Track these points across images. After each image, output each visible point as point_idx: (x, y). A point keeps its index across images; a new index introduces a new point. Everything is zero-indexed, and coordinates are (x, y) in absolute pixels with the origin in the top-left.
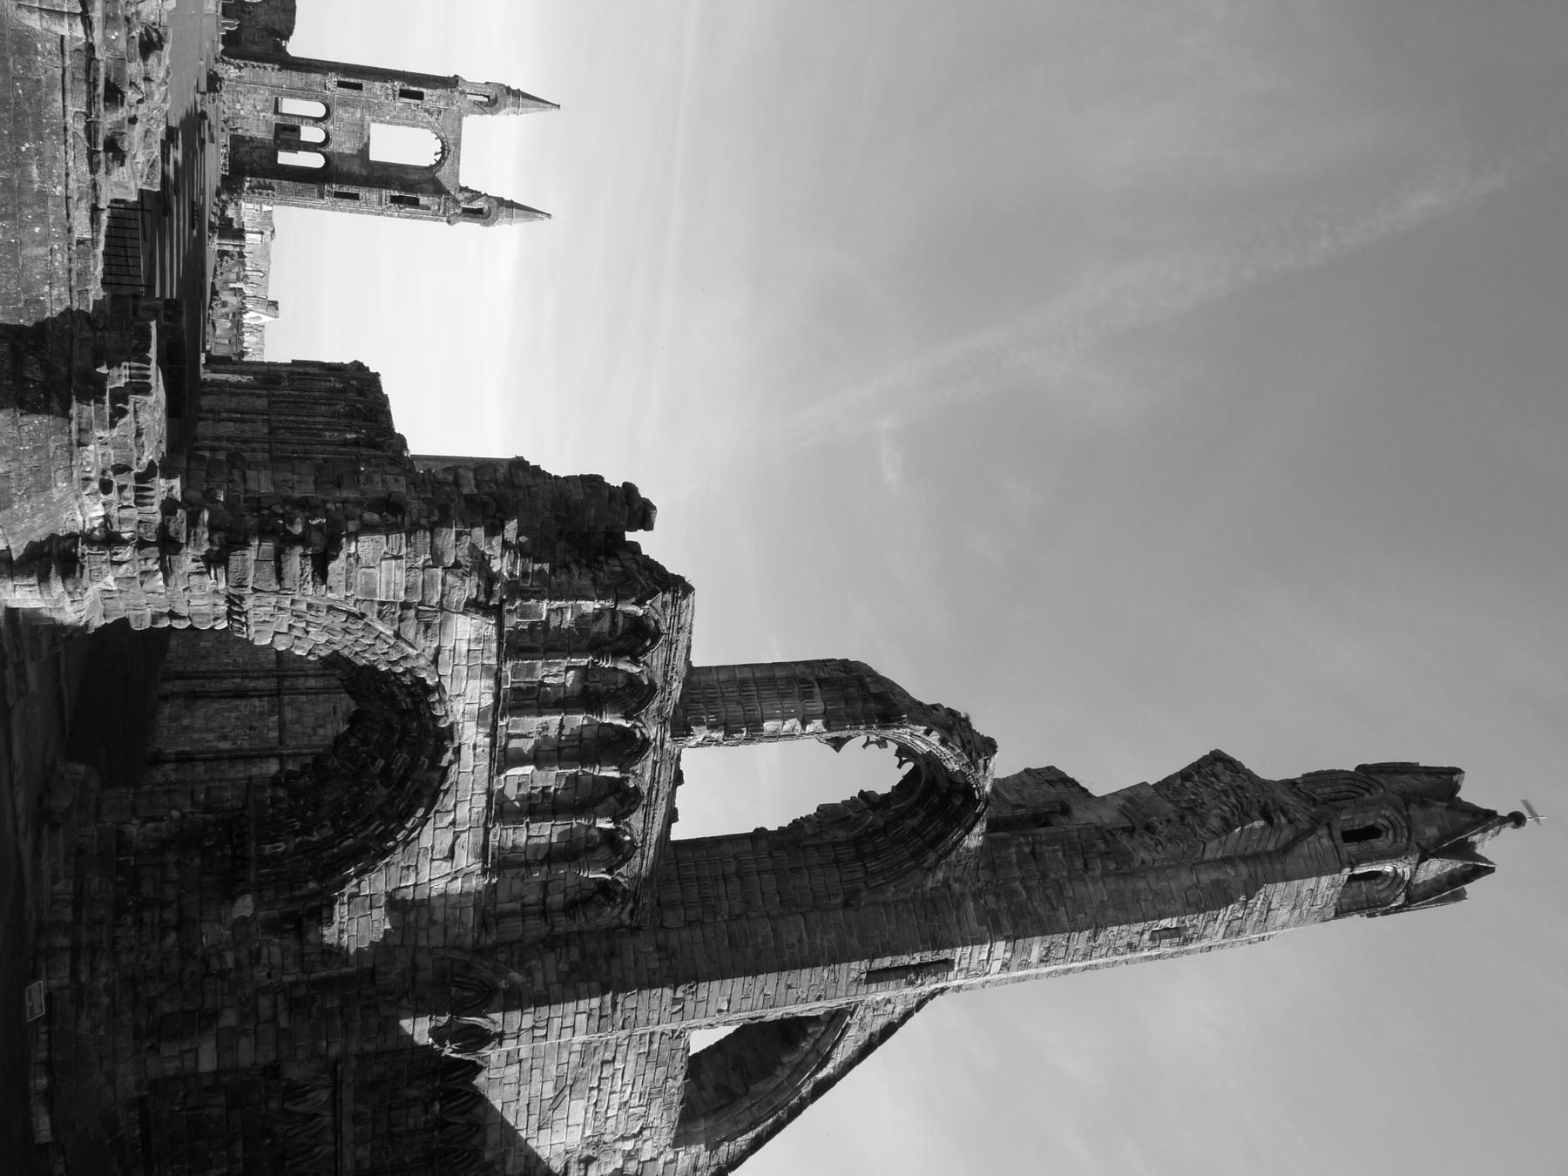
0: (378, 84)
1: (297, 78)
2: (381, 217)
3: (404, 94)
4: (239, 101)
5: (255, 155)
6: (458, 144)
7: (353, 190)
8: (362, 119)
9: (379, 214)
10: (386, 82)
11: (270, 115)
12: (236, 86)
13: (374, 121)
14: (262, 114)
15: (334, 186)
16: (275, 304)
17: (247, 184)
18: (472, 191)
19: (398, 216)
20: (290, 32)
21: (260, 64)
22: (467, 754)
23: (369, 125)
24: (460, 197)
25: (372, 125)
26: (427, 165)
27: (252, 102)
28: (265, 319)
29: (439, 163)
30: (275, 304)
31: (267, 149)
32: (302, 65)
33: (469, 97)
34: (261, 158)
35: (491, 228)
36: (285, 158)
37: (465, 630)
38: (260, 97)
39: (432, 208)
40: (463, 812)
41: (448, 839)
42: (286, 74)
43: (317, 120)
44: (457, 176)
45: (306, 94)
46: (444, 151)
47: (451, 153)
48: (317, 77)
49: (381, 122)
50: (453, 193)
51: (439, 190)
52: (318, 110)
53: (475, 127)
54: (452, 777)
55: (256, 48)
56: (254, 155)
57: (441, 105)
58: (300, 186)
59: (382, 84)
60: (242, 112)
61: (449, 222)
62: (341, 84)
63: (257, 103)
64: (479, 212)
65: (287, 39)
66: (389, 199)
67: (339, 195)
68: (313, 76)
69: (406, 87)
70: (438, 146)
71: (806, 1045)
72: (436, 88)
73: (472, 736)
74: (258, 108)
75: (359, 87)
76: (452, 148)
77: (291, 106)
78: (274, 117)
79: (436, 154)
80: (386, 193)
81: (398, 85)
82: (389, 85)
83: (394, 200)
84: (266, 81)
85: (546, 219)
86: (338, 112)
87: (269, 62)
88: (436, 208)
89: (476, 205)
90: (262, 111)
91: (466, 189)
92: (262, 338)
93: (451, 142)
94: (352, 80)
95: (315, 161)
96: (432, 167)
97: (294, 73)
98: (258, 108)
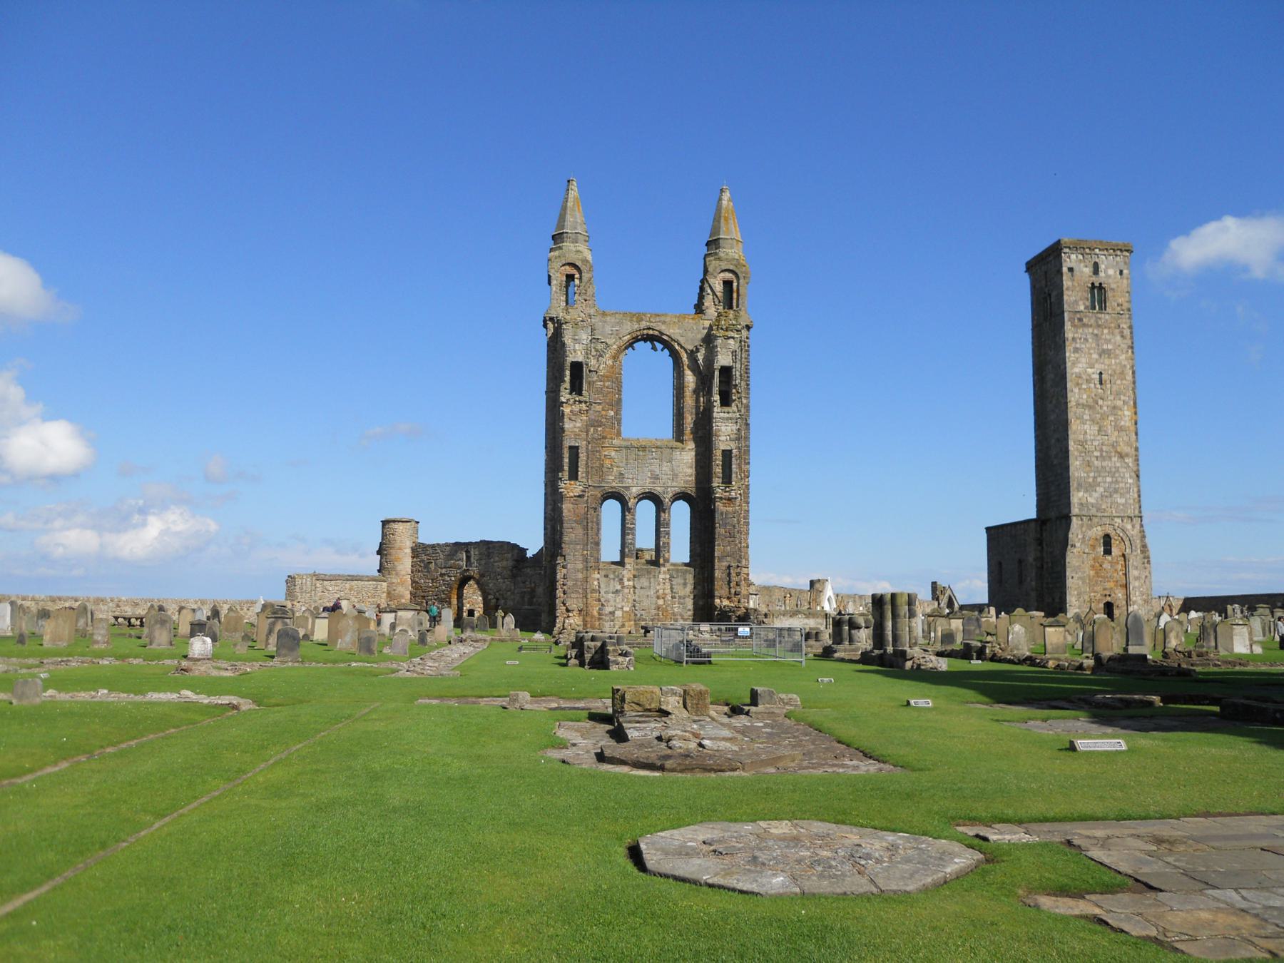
0: (568, 425)
1: (572, 534)
2: (750, 421)
3: (576, 388)
4: (612, 613)
7: (718, 456)
9: (748, 425)
10: (563, 415)
11: (627, 573)
12: (592, 616)
13: (619, 434)
14: (626, 583)
15: (715, 485)
17: (726, 602)
18: (701, 297)
19: (747, 398)
20: (515, 547)
21: (559, 585)
23: (624, 440)
24: (711, 309)
25: (625, 434)
26: (670, 360)
27: (610, 596)
28: (829, 592)
30: (812, 583)
31: (672, 576)
32: (554, 528)
34: (685, 584)
36: (680, 549)
38: (602, 586)
39: (733, 348)
42: (567, 549)
43: (625, 508)
45: (591, 526)
46: (652, 338)
47: (652, 325)
48: (567, 507)
50: (707, 324)
52: (611, 509)
55: (540, 590)
56: (682, 594)
57: (585, 336)
58: (720, 531)
59: (566, 420)
60: (626, 609)
62: (574, 476)
63: (612, 589)
64: (728, 284)
65: (524, 551)
66: (726, 409)
67: (727, 480)
68: (565, 513)
69: (567, 385)
72: (563, 345)
74: (619, 587)
75: (574, 450)
76: (644, 324)
77: (610, 550)
78: (627, 566)
79: (654, 348)
80: (718, 412)
81: (565, 396)
82: (567, 410)
83: (726, 401)
86: (612, 482)
87: (554, 573)
88: (731, 341)
89: (719, 288)
90: (621, 580)
91: (699, 308)
92: (849, 596)
93: (636, 327)
94: (566, 460)
95: (680, 515)
96: (675, 355)
97: (566, 538)
98: (619, 587)
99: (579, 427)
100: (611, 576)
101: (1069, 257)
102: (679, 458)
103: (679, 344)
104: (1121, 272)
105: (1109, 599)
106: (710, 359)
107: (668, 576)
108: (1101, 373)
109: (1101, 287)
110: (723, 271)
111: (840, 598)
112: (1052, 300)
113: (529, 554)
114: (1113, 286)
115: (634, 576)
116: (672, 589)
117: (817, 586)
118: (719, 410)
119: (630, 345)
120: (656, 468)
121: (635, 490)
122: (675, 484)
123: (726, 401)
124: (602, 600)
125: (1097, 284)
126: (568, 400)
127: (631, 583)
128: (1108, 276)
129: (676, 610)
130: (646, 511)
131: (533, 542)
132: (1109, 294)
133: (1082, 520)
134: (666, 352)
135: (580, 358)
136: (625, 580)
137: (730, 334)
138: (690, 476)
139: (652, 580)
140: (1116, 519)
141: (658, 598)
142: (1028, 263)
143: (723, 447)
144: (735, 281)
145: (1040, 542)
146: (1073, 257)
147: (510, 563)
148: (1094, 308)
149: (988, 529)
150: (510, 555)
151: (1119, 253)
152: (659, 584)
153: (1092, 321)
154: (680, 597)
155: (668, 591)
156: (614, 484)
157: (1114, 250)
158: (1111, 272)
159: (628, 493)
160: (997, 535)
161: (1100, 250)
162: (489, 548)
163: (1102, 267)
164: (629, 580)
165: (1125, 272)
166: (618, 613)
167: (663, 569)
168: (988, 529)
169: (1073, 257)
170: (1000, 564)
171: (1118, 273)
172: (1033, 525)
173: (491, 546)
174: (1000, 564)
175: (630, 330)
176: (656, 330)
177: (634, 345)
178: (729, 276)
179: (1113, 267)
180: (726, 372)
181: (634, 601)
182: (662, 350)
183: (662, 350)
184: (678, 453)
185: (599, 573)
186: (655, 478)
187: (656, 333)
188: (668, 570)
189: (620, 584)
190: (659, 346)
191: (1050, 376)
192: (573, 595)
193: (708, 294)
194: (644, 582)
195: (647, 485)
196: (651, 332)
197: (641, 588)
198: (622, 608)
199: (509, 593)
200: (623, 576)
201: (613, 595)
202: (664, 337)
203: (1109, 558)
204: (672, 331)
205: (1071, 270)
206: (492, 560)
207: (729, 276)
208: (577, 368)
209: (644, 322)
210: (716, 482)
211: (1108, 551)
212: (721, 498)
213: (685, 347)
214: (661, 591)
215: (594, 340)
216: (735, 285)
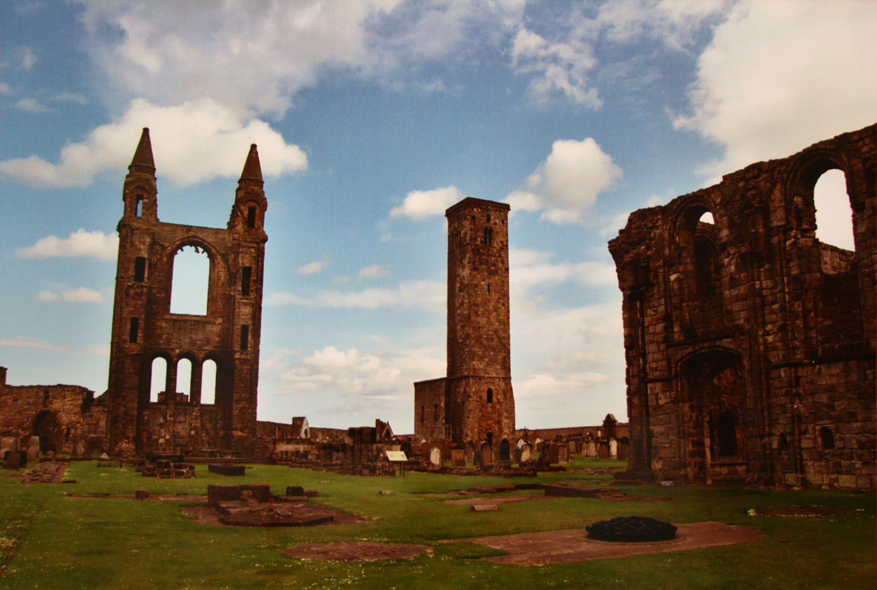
3: (139, 277)
4: (157, 440)
5: (209, 426)
6: (189, 228)
8: (167, 321)
14: (168, 418)
16: (295, 419)
17: (240, 433)
20: (83, 390)
26: (208, 260)
27: (157, 428)
29: (206, 249)
30: (295, 419)
33: (139, 214)
35: (268, 201)
36: (208, 396)
44: (217, 231)
49: (169, 303)
51: (236, 248)
53: (167, 214)
60: (168, 437)
61: (265, 240)
62: (133, 339)
64: (252, 211)
65: (92, 393)
67: (244, 346)
70: (189, 250)
74: (162, 421)
76: (191, 233)
79: (197, 251)
84: (135, 412)
85: (258, 149)
88: (253, 250)
89: (246, 213)
90: (165, 418)
91: (231, 224)
93: (186, 235)
95: (210, 368)
96: (211, 256)
98: (162, 421)
99: (140, 305)
100: (158, 413)
101: (473, 210)
102: (210, 328)
103: (216, 250)
104: (503, 223)
105: (490, 431)
106: (236, 260)
107: (199, 414)
108: (489, 286)
110: (251, 200)
111: (313, 430)
112: (462, 236)
113: (96, 396)
114: (498, 230)
115: (175, 414)
116: (202, 423)
117: (299, 423)
118: (241, 297)
119: (180, 247)
120: (194, 337)
121: (177, 351)
122: (206, 348)
123: (245, 292)
124: (150, 430)
125: (489, 228)
126: (134, 284)
127: (172, 419)
128: (495, 224)
129: (204, 438)
130: (184, 367)
131: (99, 386)
132: (494, 235)
133: (475, 379)
134: (206, 254)
136: (168, 416)
137: (251, 245)
138: (218, 342)
139: (187, 416)
140: (496, 380)
141: (191, 429)
142: (447, 211)
143: (242, 323)
144: (258, 208)
145: (447, 394)
146: (475, 210)
147: (80, 402)
148: (485, 243)
149: (416, 384)
150: (81, 397)
151: (502, 210)
152: (192, 419)
153: (485, 252)
154: (207, 429)
155: (199, 425)
156: (162, 347)
157: (500, 208)
158: (497, 221)
159: (173, 353)
160: (420, 387)
161: (491, 207)
162: (64, 391)
164: (170, 416)
165: (505, 222)
166: (161, 441)
167: (195, 409)
168: (416, 384)
169: (475, 210)
170: (423, 408)
171: (501, 222)
172: (444, 382)
173: (66, 389)
174: (423, 408)
175: (181, 237)
176: (200, 238)
177: (184, 248)
178: (253, 204)
179: (499, 218)
180: (247, 271)
181: (174, 431)
182: (203, 252)
183: (203, 252)
184: (210, 326)
185: (148, 411)
186: (193, 343)
187: (200, 240)
188: (200, 410)
189: (164, 419)
190: (201, 250)
191: (458, 285)
192: (129, 427)
193: (238, 216)
194: (181, 418)
195: (186, 347)
196: (196, 240)
197: (180, 422)
198: (164, 437)
199: (78, 425)
200: (167, 414)
201: (159, 427)
202: (205, 243)
203: (490, 404)
204: (210, 239)
205: (473, 218)
206: (66, 400)
207: (253, 204)
208: (140, 262)
209: (191, 232)
210: (237, 348)
211: (490, 399)
212: (240, 359)
213: (220, 251)
214: (193, 425)
215: (153, 243)
216: (257, 211)
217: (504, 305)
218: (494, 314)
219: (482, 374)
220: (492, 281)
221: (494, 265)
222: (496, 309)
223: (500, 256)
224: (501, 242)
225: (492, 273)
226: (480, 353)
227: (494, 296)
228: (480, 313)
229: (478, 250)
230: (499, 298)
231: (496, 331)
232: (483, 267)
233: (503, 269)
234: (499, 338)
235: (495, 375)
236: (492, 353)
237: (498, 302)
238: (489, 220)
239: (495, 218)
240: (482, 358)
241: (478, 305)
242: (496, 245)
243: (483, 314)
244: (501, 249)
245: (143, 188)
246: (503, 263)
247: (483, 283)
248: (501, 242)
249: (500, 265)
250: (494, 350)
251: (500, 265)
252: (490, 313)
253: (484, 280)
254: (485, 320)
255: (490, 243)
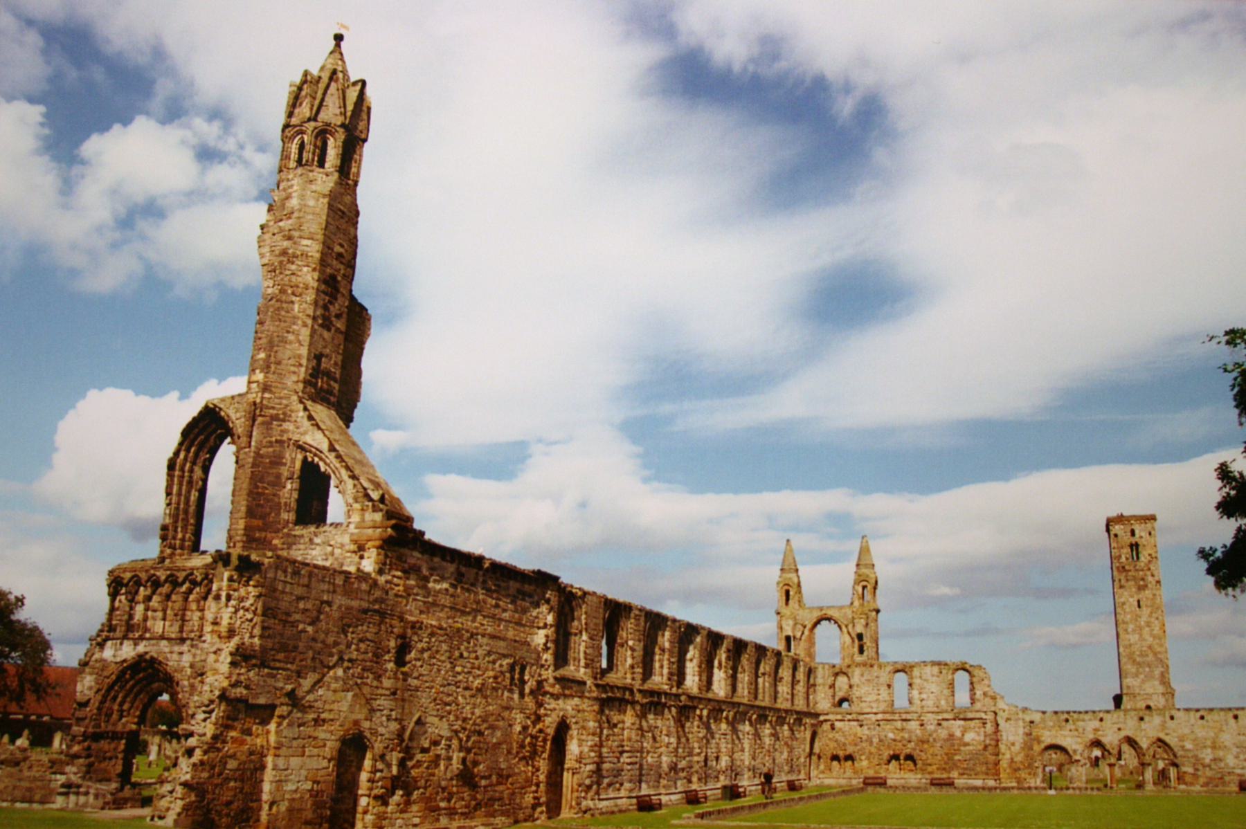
22: (147, 649)
37: (108, 653)
40: (167, 650)
41: (175, 656)
54: (155, 655)
57: (791, 622)
71: (316, 459)
73: (141, 648)
76: (824, 612)
108: (1139, 601)
109: (1137, 545)
128: (1141, 537)
132: (1140, 549)
135: (790, 633)
153: (1132, 568)
158: (1143, 534)
163: (1137, 532)
169: (1117, 527)
207: (864, 583)
217: (1157, 618)
218: (1147, 629)
219: (1137, 691)
220: (1140, 596)
221: (1143, 579)
222: (1148, 624)
223: (1149, 569)
224: (1150, 555)
225: (1141, 588)
226: (1134, 670)
227: (1145, 611)
228: (1130, 630)
229: (1123, 567)
230: (1151, 613)
231: (1150, 647)
232: (1131, 583)
233: (1154, 583)
234: (1155, 654)
235: (1151, 691)
236: (1147, 669)
237: (1150, 616)
238: (1133, 533)
239: (1140, 531)
240: (1136, 675)
241: (1127, 623)
242: (1144, 558)
243: (1134, 631)
244: (1150, 562)
245: (788, 585)
246: (1153, 575)
247: (1131, 600)
248: (1150, 555)
249: (1150, 578)
250: (1149, 666)
251: (1150, 578)
252: (1141, 628)
253: (1132, 596)
254: (1137, 636)
255: (1138, 558)
